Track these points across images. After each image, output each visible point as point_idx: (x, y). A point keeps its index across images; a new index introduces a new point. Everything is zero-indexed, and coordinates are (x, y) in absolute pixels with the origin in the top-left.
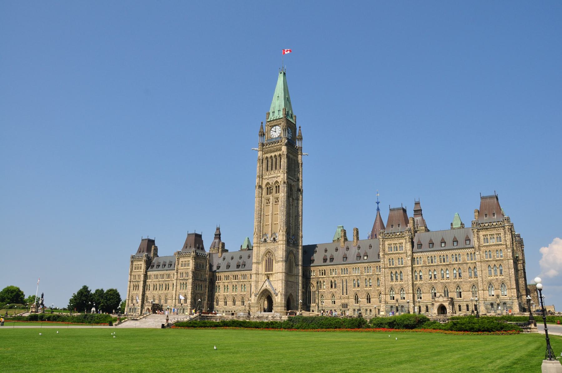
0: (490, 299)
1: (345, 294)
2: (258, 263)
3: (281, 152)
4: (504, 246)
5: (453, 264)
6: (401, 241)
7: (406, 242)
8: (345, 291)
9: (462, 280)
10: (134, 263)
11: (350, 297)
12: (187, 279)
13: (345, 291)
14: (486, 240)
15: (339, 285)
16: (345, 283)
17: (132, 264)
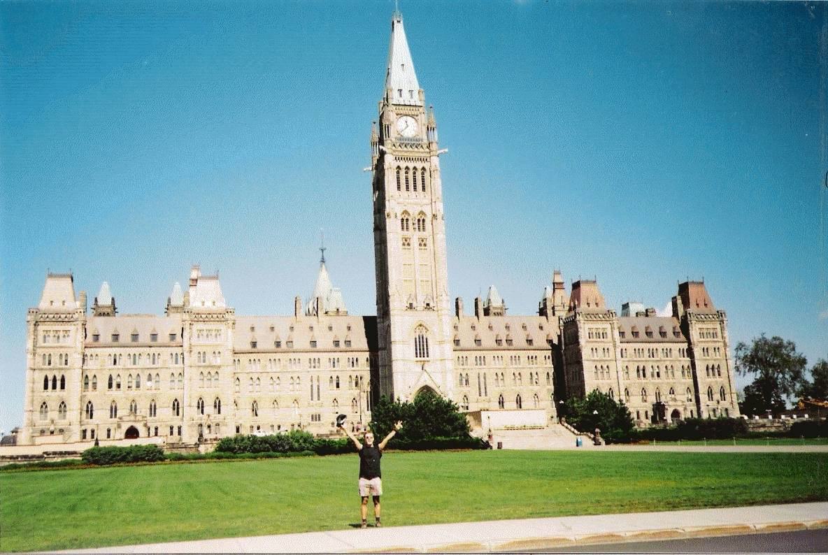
0: (713, 404)
1: (483, 394)
2: (404, 342)
3: (426, 165)
4: (722, 344)
5: (664, 361)
6: (604, 326)
7: (612, 328)
8: (483, 390)
9: (674, 381)
10: (41, 328)
11: (492, 399)
12: (219, 367)
13: (483, 390)
14: (702, 335)
15: (473, 380)
16: (482, 379)
17: (35, 330)
